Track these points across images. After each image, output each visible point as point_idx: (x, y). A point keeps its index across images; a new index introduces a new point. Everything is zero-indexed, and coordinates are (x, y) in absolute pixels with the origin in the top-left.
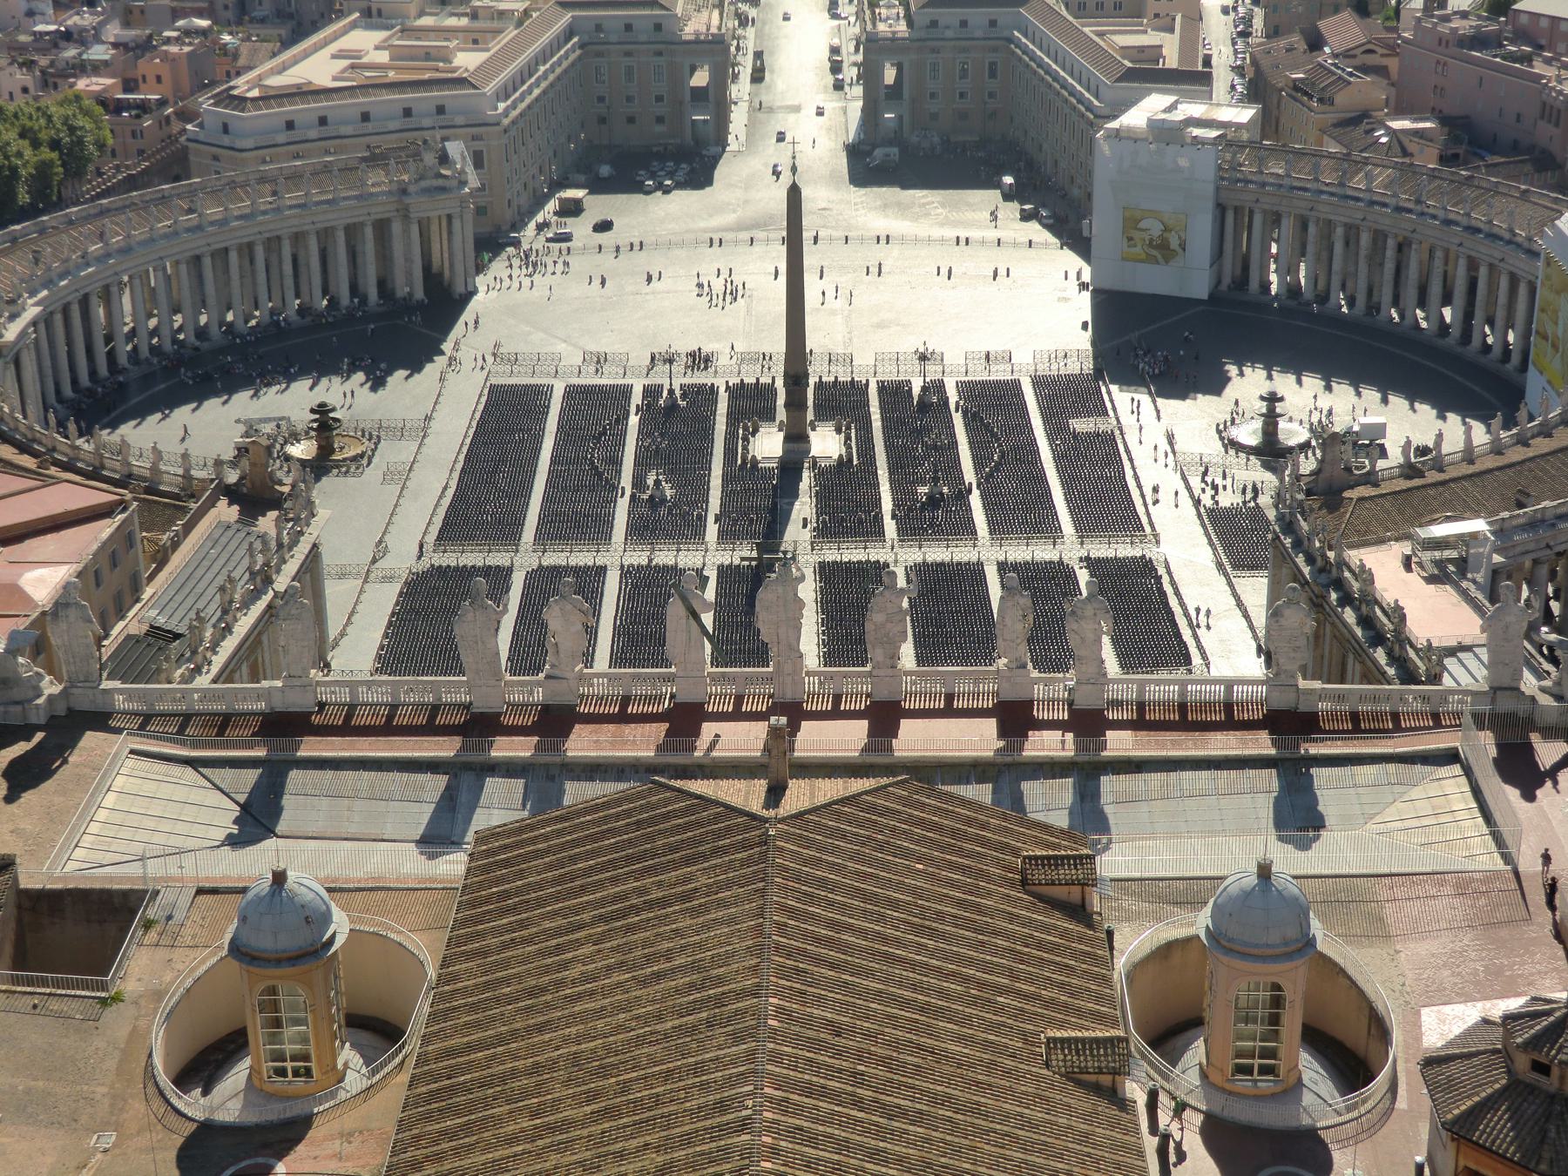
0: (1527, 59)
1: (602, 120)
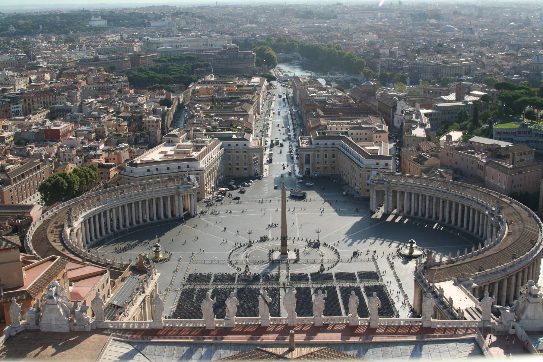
0: (473, 153)
1: (230, 169)
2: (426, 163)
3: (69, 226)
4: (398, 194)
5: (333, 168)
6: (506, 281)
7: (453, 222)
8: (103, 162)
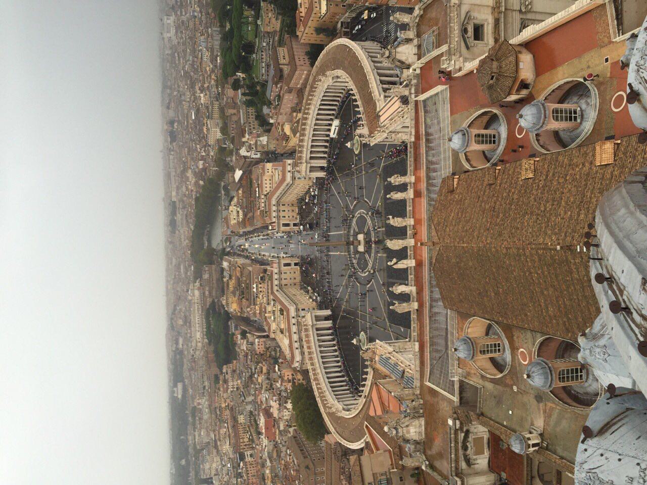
3: (341, 412)
4: (312, 155)
6: (379, 71)
8: (291, 384)
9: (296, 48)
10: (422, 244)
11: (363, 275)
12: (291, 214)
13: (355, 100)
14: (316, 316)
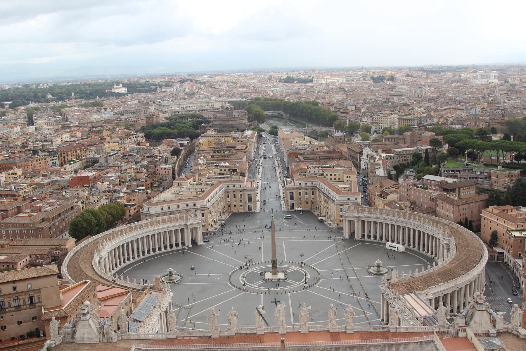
2: (388, 197)
4: (366, 223)
5: (313, 203)
7: (411, 246)
9: (476, 206)
10: (283, 342)
11: (240, 278)
12: (303, 201)
13: (426, 268)
14: (196, 228)
